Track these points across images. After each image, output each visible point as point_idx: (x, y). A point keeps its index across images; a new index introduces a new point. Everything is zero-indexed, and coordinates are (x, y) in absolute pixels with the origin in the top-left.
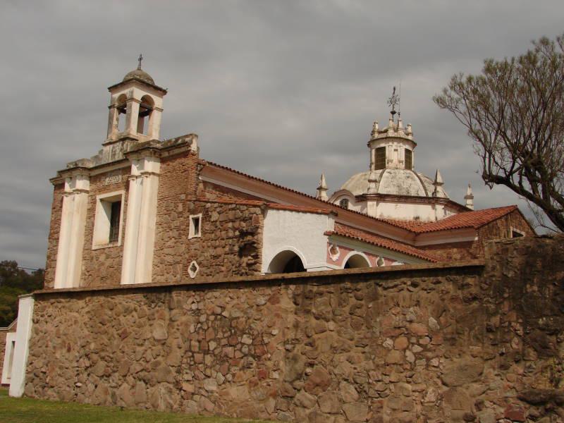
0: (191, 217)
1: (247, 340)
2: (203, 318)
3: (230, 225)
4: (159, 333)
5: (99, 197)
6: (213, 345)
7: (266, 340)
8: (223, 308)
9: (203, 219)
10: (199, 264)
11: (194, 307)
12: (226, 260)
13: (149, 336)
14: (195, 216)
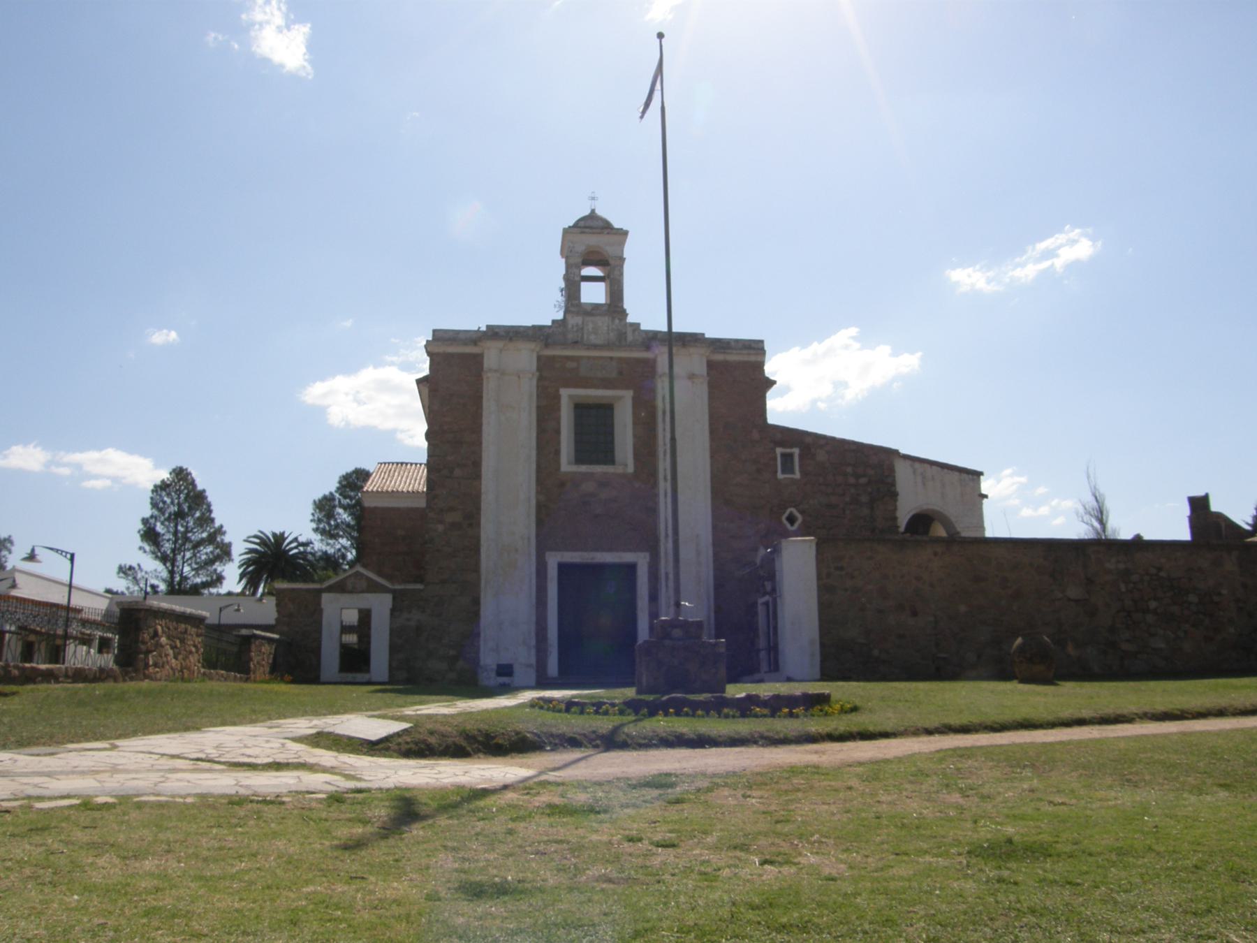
0: (779, 450)
1: (1193, 598)
2: (1135, 578)
3: (849, 470)
4: (1074, 592)
5: (565, 393)
6: (1153, 605)
7: (1216, 599)
8: (1160, 569)
9: (801, 456)
10: (802, 512)
11: (1121, 566)
12: (848, 512)
13: (1060, 595)
14: (788, 450)
